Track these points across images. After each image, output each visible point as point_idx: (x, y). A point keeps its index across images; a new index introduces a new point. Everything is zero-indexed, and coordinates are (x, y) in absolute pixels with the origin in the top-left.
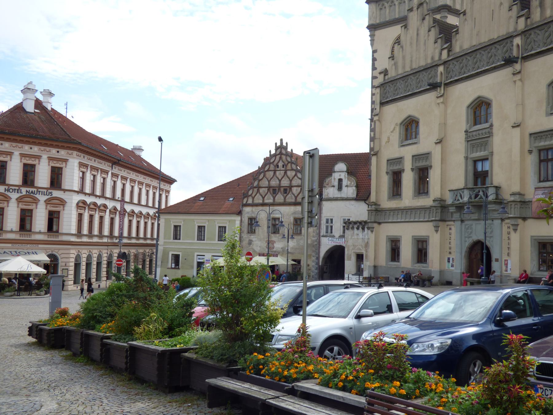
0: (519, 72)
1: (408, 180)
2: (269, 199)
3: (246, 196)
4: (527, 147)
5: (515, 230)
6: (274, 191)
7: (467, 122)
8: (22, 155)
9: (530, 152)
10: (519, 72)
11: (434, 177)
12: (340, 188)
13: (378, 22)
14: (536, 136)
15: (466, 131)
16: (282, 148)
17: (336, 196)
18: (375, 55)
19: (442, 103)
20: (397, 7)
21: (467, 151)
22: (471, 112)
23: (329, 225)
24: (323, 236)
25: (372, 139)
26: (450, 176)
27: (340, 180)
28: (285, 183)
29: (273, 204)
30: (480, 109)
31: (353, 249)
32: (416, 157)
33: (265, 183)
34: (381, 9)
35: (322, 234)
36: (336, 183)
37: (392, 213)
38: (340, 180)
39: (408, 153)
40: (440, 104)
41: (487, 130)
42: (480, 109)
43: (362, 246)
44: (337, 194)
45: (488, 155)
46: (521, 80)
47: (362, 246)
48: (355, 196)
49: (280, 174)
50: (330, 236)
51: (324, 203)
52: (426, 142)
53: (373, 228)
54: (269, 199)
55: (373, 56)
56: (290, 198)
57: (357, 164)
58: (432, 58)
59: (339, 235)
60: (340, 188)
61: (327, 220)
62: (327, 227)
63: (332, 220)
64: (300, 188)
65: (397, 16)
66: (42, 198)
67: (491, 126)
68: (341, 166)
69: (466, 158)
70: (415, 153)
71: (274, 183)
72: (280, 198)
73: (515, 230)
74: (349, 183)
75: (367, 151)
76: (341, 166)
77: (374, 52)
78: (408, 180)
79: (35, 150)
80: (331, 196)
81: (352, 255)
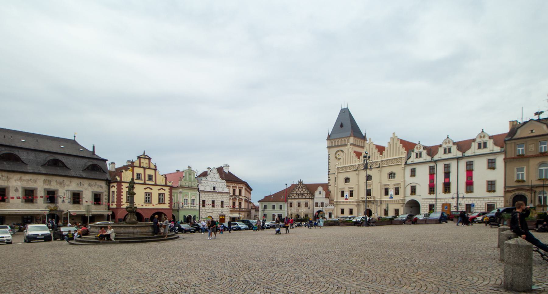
2: (297, 197)
3: (289, 196)
6: (299, 195)
8: (233, 187)
12: (320, 193)
16: (300, 182)
25: (329, 180)
28: (302, 192)
29: (298, 199)
33: (295, 192)
49: (300, 190)
52: (352, 184)
54: (297, 197)
56: (304, 197)
57: (325, 187)
60: (320, 193)
66: (238, 198)
68: (320, 189)
71: (298, 192)
72: (300, 197)
75: (327, 182)
76: (320, 189)
79: (235, 185)
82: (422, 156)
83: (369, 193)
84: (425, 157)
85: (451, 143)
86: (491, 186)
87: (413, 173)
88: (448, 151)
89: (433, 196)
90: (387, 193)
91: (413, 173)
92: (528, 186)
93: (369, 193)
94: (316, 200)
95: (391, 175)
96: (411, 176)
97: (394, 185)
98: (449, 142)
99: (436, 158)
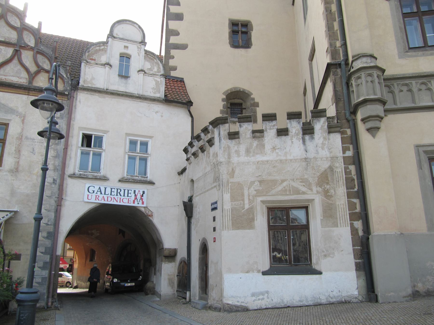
24: (73, 176)
31: (259, 193)
35: (70, 170)
36: (115, 61)
43: (304, 181)
44: (118, 85)
47: (304, 181)
48: (161, 94)
50: (96, 178)
51: (81, 97)
59: (120, 177)
64: (9, 51)
80: (100, 84)
81: (259, 208)
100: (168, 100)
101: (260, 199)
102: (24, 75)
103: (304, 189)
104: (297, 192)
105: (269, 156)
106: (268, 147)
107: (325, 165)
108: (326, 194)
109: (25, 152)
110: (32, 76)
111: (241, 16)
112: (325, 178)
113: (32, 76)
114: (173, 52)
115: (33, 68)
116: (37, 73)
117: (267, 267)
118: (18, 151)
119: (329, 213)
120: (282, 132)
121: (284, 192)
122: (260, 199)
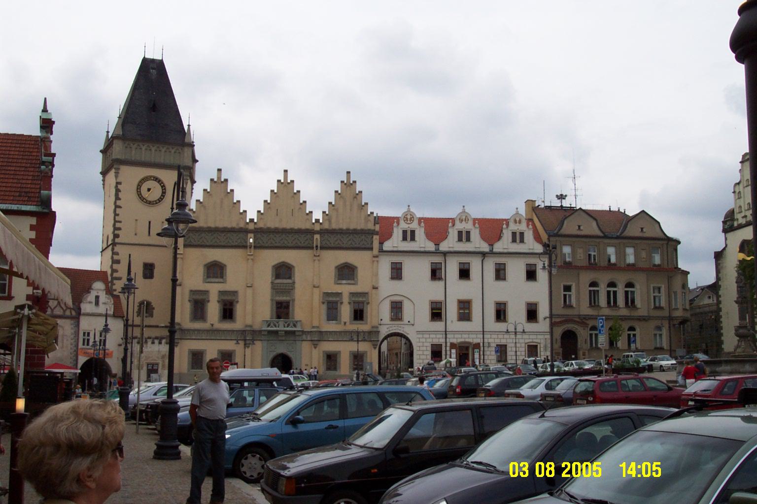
0: (319, 256)
1: (213, 310)
4: (321, 300)
5: (315, 348)
7: (272, 277)
9: (323, 303)
10: (319, 256)
11: (239, 310)
13: (123, 158)
14: (327, 294)
15: (272, 283)
17: (94, 312)
18: (119, 186)
19: (252, 259)
20: (143, 152)
21: (272, 296)
22: (274, 270)
23: (86, 337)
26: (255, 309)
27: (97, 297)
30: (283, 271)
31: (145, 360)
32: (221, 293)
34: (126, 147)
36: (93, 300)
37: (211, 333)
38: (97, 297)
39: (214, 289)
40: (250, 261)
41: (290, 285)
42: (283, 271)
45: (290, 300)
46: (319, 260)
53: (178, 343)
55: (116, 187)
58: (238, 224)
60: (97, 303)
61: (84, 333)
62: (84, 340)
63: (89, 334)
65: (143, 160)
67: (294, 283)
68: (99, 286)
69: (272, 300)
70: (222, 290)
73: (315, 348)
74: (107, 300)
76: (99, 286)
77: (118, 183)
78: (213, 310)
82: (417, 238)
83: (282, 309)
84: (422, 242)
85: (471, 222)
86: (532, 314)
87: (397, 273)
88: (465, 236)
89: (439, 326)
90: (332, 312)
91: (397, 273)
92: (579, 316)
93: (282, 309)
94: (85, 324)
95: (346, 272)
96: (393, 278)
97: (353, 294)
98: (467, 220)
99: (444, 246)
100: (115, 316)
101: (146, 361)
102: (62, 311)
103: (157, 359)
104: (155, 360)
105: (150, 350)
106: (148, 348)
107: (164, 353)
108: (163, 362)
109: (65, 341)
110: (64, 311)
111: (149, 261)
112: (163, 357)
113: (64, 311)
114: (115, 281)
115: (65, 308)
116: (66, 310)
117: (146, 380)
118: (63, 340)
119: (163, 366)
120: (153, 343)
121: (152, 360)
122: (146, 361)
